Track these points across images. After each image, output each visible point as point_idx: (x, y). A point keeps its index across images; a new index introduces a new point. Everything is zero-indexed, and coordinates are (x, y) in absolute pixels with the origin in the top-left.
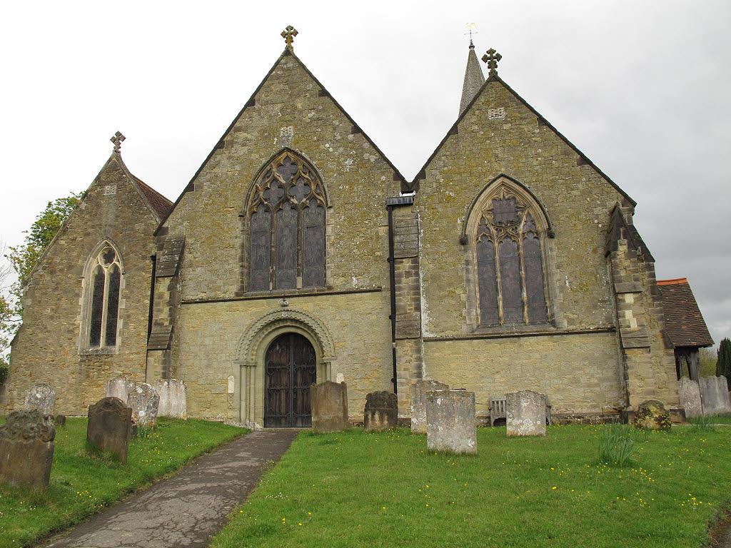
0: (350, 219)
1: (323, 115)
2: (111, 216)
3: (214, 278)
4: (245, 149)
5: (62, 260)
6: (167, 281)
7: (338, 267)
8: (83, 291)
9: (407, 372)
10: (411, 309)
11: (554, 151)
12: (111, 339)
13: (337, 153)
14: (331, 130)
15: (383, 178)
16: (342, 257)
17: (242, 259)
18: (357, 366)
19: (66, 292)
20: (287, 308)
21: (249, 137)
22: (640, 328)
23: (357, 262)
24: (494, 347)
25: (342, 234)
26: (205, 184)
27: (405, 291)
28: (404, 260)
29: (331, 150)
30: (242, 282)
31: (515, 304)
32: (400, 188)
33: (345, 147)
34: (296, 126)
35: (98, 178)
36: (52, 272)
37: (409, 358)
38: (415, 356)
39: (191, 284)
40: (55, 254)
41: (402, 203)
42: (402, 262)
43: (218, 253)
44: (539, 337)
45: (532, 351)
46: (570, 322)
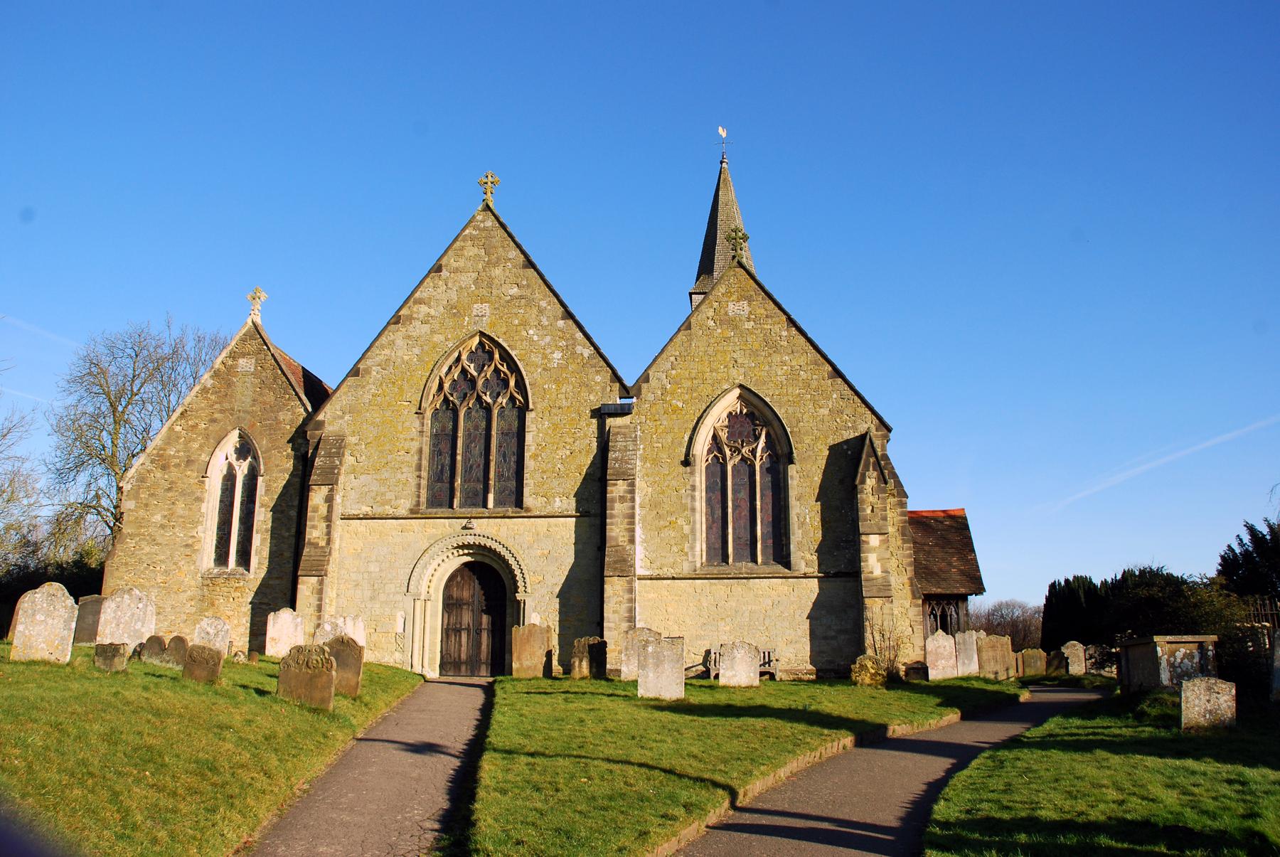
0: (555, 427)
1: (527, 293)
4: (426, 328)
5: (178, 451)
6: (325, 490)
9: (616, 615)
14: (535, 311)
15: (598, 378)
19: (183, 493)
21: (432, 312)
24: (720, 587)
26: (374, 368)
29: (535, 338)
36: (164, 468)
38: (627, 596)
42: (616, 485)
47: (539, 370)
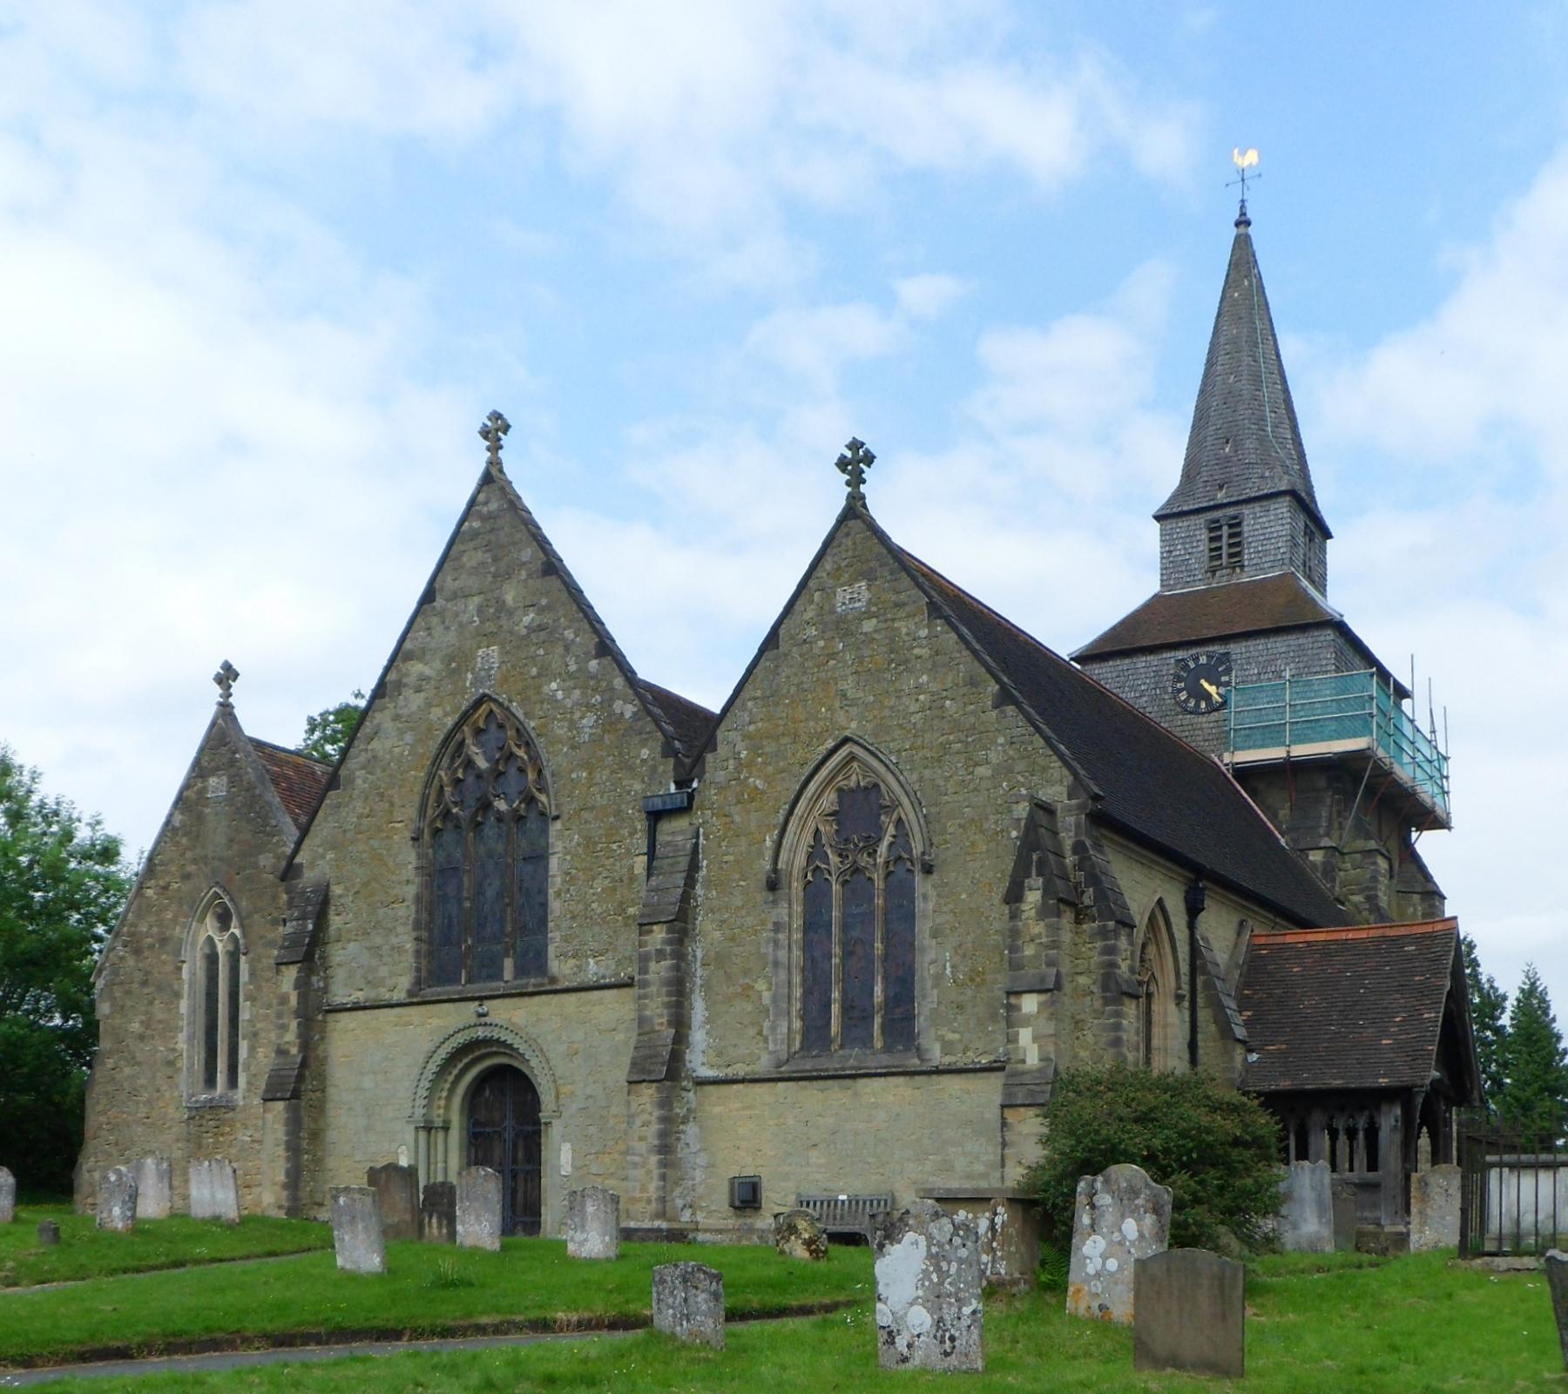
1: (547, 619)
2: (221, 839)
3: (374, 963)
5: (151, 927)
7: (566, 939)
8: (186, 987)
9: (643, 1143)
10: (662, 1024)
11: (950, 678)
12: (233, 1082)
13: (569, 703)
14: (560, 650)
15: (645, 753)
16: (573, 918)
17: (417, 925)
18: (592, 1130)
20: (487, 1020)
21: (427, 671)
22: (1042, 1064)
23: (597, 929)
24: (810, 1096)
25: (574, 871)
27: (653, 989)
28: (655, 927)
29: (560, 695)
30: (418, 970)
31: (856, 1014)
32: (671, 774)
33: (584, 688)
34: (502, 645)
35: (197, 763)
36: (137, 952)
37: (646, 1117)
39: (339, 975)
40: (139, 916)
41: (669, 807)
42: (651, 931)
43: (381, 912)
44: (890, 1079)
45: (876, 1106)
46: (947, 1047)
47: (565, 750)
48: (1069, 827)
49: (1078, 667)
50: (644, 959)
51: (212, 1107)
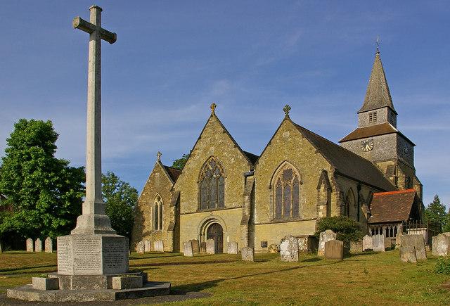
12: (161, 228)
31: (287, 211)
48: (330, 176)
49: (340, 144)
50: (244, 203)
51: (157, 233)
